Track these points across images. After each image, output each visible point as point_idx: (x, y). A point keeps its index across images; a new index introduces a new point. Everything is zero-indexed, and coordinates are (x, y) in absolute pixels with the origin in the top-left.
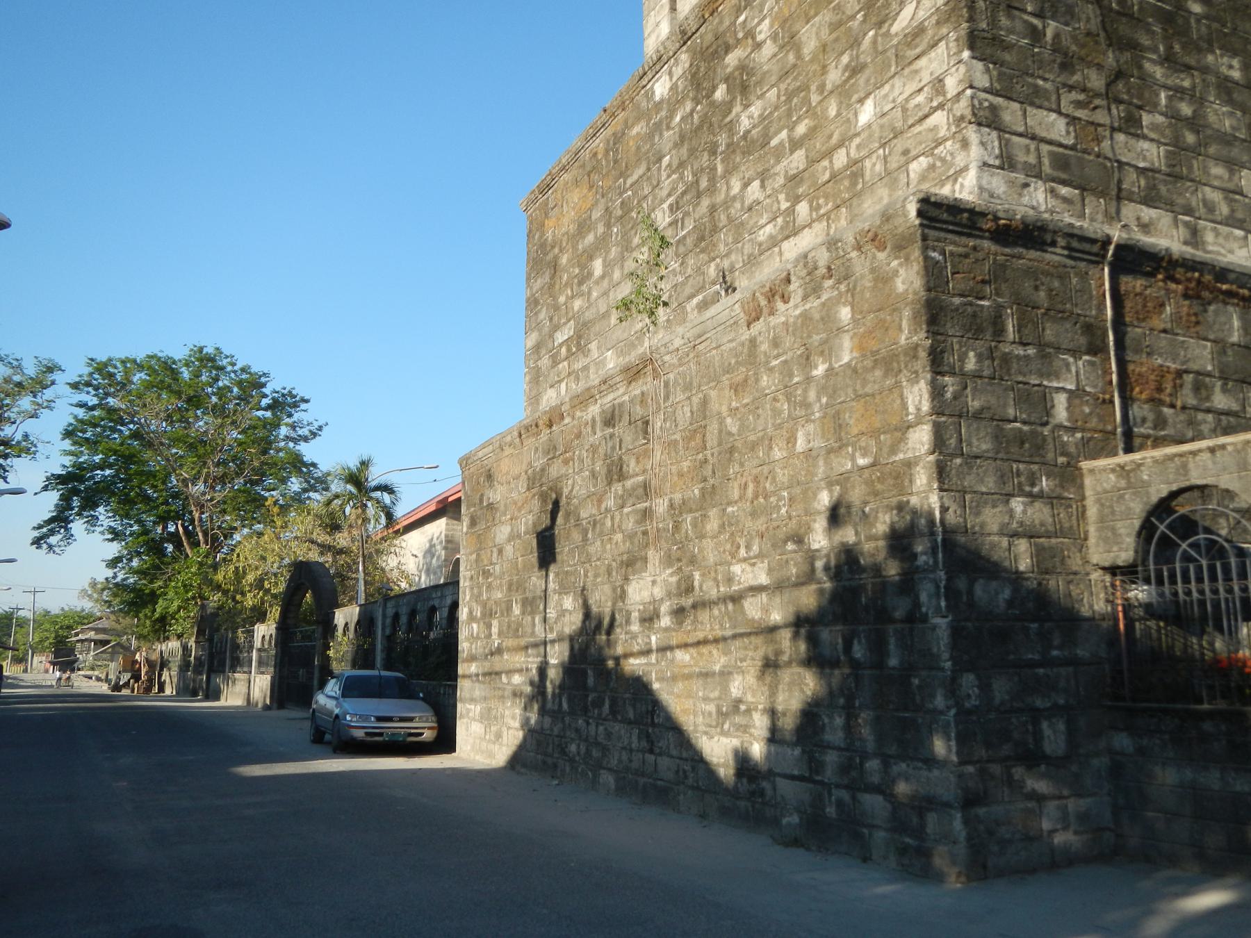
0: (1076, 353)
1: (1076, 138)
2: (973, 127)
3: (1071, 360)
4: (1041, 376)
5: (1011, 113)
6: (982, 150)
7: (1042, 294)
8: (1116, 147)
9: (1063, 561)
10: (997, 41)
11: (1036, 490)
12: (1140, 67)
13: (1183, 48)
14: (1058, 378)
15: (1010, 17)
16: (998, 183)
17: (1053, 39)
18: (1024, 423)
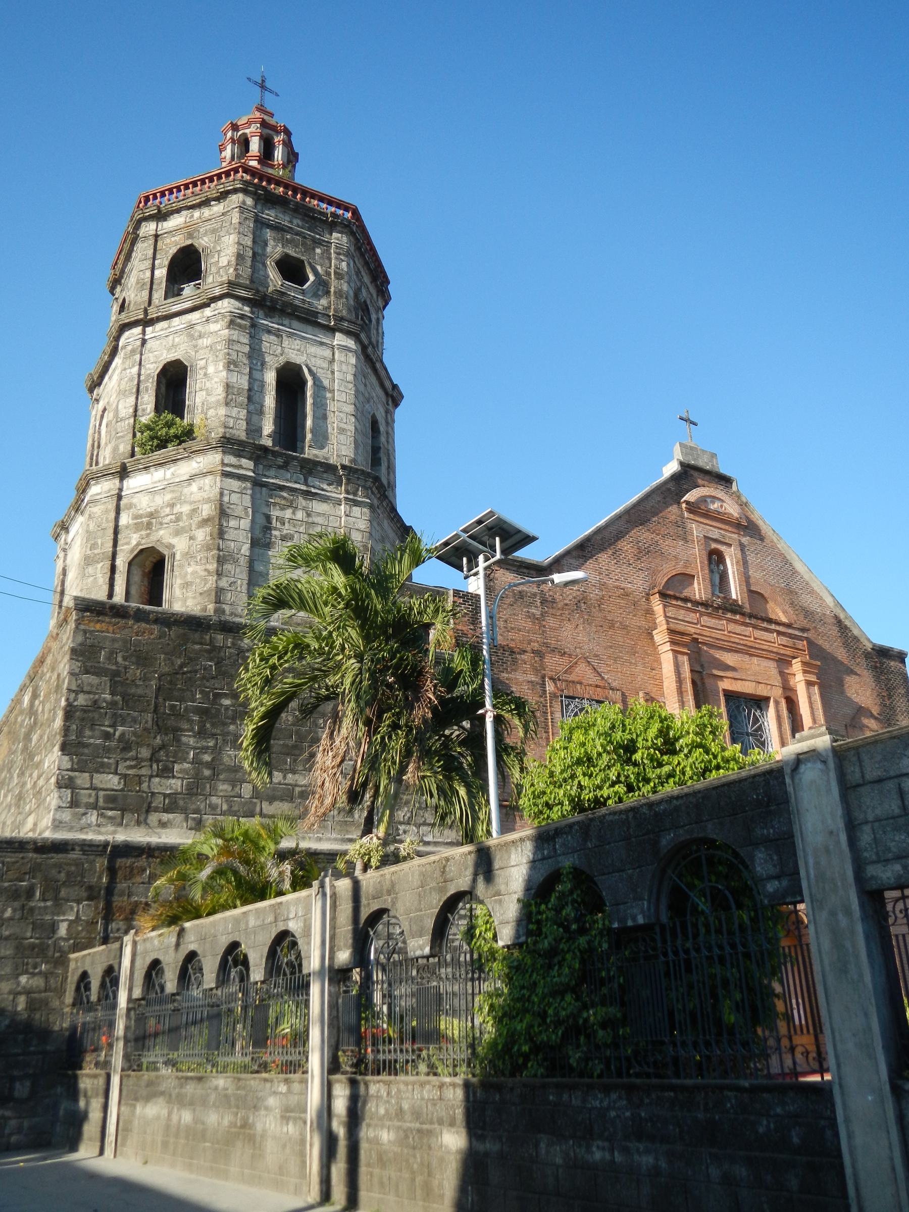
0: (78, 902)
1: (125, 785)
2: (56, 790)
3: (75, 905)
4: (53, 914)
5: (83, 779)
6: (59, 801)
7: (63, 875)
8: (152, 786)
9: (47, 1004)
11: (37, 971)
12: (179, 741)
13: (213, 725)
14: (64, 914)
15: (92, 729)
16: (66, 816)
17: (120, 737)
18: (37, 938)
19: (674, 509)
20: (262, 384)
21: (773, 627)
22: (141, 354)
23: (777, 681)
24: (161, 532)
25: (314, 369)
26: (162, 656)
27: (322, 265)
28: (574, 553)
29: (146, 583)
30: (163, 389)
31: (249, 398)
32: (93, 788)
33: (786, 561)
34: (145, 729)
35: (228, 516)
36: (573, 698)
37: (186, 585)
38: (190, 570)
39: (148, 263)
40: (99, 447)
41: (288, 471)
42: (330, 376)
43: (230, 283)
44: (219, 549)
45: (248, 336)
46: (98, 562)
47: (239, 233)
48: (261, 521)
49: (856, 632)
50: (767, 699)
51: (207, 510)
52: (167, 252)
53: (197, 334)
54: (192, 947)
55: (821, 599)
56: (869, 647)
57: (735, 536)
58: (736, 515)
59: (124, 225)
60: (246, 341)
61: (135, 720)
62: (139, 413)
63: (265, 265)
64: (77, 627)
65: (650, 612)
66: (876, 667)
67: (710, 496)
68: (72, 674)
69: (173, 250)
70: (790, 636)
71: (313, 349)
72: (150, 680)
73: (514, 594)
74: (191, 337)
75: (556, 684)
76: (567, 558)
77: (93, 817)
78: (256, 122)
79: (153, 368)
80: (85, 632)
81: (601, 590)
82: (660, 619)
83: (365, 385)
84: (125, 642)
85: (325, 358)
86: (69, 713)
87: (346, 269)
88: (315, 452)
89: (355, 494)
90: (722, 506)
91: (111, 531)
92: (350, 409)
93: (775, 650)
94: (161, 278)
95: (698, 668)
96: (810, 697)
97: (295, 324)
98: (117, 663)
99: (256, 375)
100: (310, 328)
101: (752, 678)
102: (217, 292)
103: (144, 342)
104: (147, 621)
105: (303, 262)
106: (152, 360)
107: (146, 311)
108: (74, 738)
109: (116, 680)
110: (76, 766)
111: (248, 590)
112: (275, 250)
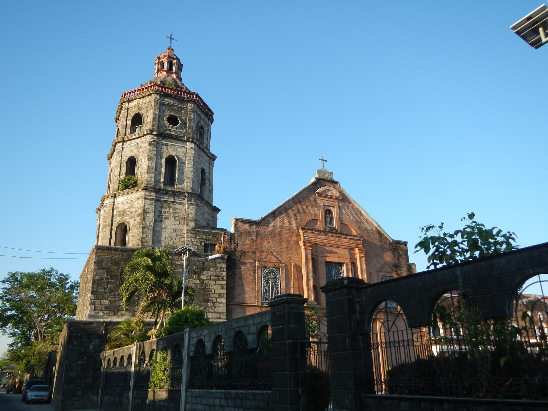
5: (98, 302)
10: (97, 291)
14: (91, 343)
15: (100, 286)
19: (313, 196)
20: (161, 164)
21: (348, 237)
22: (122, 153)
23: (348, 257)
24: (126, 217)
25: (179, 156)
26: (123, 262)
27: (184, 117)
28: (270, 216)
29: (122, 233)
30: (129, 165)
31: (156, 170)
32: (101, 304)
33: (358, 211)
34: (117, 286)
35: (146, 213)
36: (266, 267)
37: (133, 236)
38: (134, 231)
39: (125, 119)
40: (110, 182)
41: (167, 195)
42: (185, 158)
43: (150, 130)
44: (143, 224)
45: (156, 148)
46: (107, 227)
47: (154, 109)
48: (158, 213)
49: (386, 236)
50: (344, 263)
51: (140, 211)
52: (131, 115)
53: (139, 147)
54: (116, 356)
55: (372, 224)
56: (391, 241)
57: (337, 204)
58: (338, 196)
59: (117, 104)
60: (155, 149)
61: (114, 283)
62: (121, 174)
63: (163, 120)
64: (96, 255)
65: (299, 235)
66: (394, 248)
67: (327, 190)
68: (95, 270)
69: (133, 114)
70: (355, 240)
71: (179, 149)
72: (119, 270)
73: (246, 232)
74: (137, 147)
75: (260, 263)
76: (268, 218)
77: (101, 313)
78: (166, 57)
79: (125, 158)
80: (98, 256)
81: (280, 228)
82: (302, 238)
83: (199, 158)
84: (111, 258)
85: (183, 152)
86: (93, 282)
87: (192, 117)
88: (178, 186)
89: (191, 201)
90: (332, 193)
91: (111, 216)
92: (191, 170)
93: (348, 245)
94: (129, 124)
95: (316, 254)
96: (361, 262)
97: (173, 140)
98: (108, 265)
99: (159, 161)
100: (178, 142)
101: (338, 256)
102: (146, 133)
103: (123, 148)
104: (118, 251)
105: (177, 117)
106: (125, 155)
107: (123, 138)
108: (95, 289)
109: (108, 271)
110: (95, 298)
111: (153, 237)
112: (168, 114)
